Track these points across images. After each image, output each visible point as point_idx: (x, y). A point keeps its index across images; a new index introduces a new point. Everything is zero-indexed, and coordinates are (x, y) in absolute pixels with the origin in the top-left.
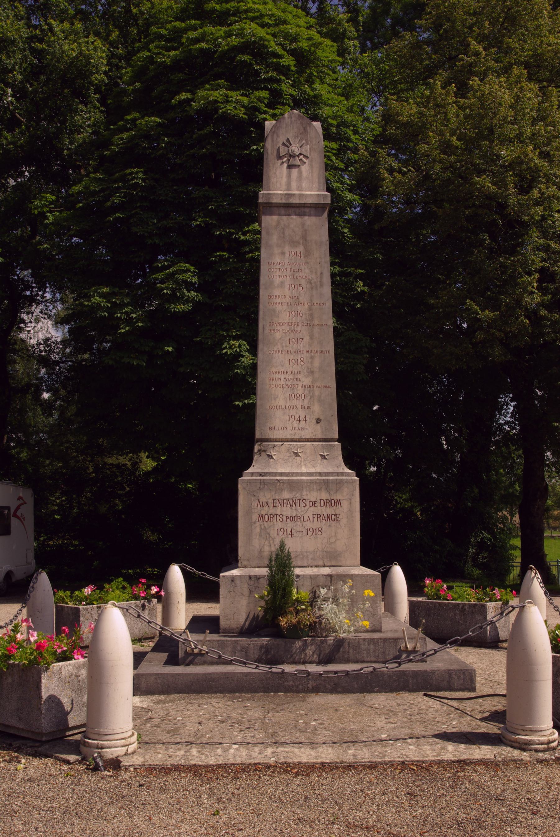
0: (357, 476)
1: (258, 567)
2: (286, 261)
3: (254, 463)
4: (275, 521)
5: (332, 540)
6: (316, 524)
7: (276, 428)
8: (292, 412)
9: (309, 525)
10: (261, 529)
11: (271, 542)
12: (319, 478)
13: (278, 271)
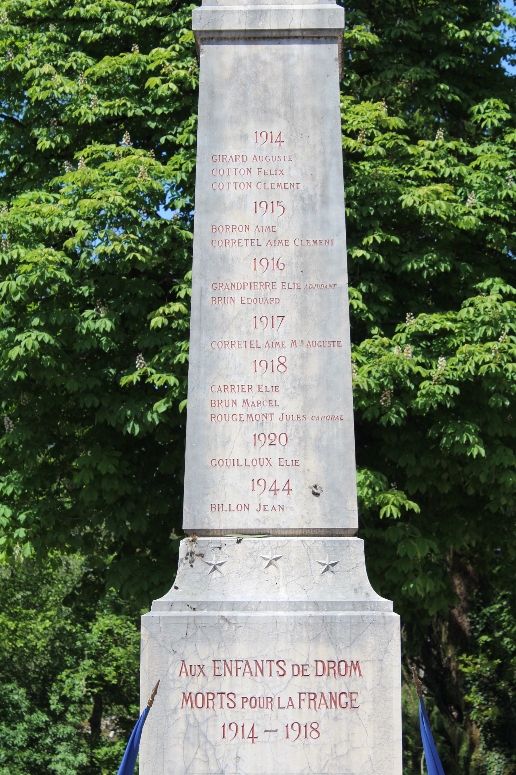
0: (395, 610)
3: (176, 583)
4: (217, 706)
5: (342, 750)
6: (306, 715)
7: (226, 507)
8: (259, 473)
9: (291, 715)
10: (188, 724)
11: (210, 753)
12: (313, 613)
13: (232, 173)
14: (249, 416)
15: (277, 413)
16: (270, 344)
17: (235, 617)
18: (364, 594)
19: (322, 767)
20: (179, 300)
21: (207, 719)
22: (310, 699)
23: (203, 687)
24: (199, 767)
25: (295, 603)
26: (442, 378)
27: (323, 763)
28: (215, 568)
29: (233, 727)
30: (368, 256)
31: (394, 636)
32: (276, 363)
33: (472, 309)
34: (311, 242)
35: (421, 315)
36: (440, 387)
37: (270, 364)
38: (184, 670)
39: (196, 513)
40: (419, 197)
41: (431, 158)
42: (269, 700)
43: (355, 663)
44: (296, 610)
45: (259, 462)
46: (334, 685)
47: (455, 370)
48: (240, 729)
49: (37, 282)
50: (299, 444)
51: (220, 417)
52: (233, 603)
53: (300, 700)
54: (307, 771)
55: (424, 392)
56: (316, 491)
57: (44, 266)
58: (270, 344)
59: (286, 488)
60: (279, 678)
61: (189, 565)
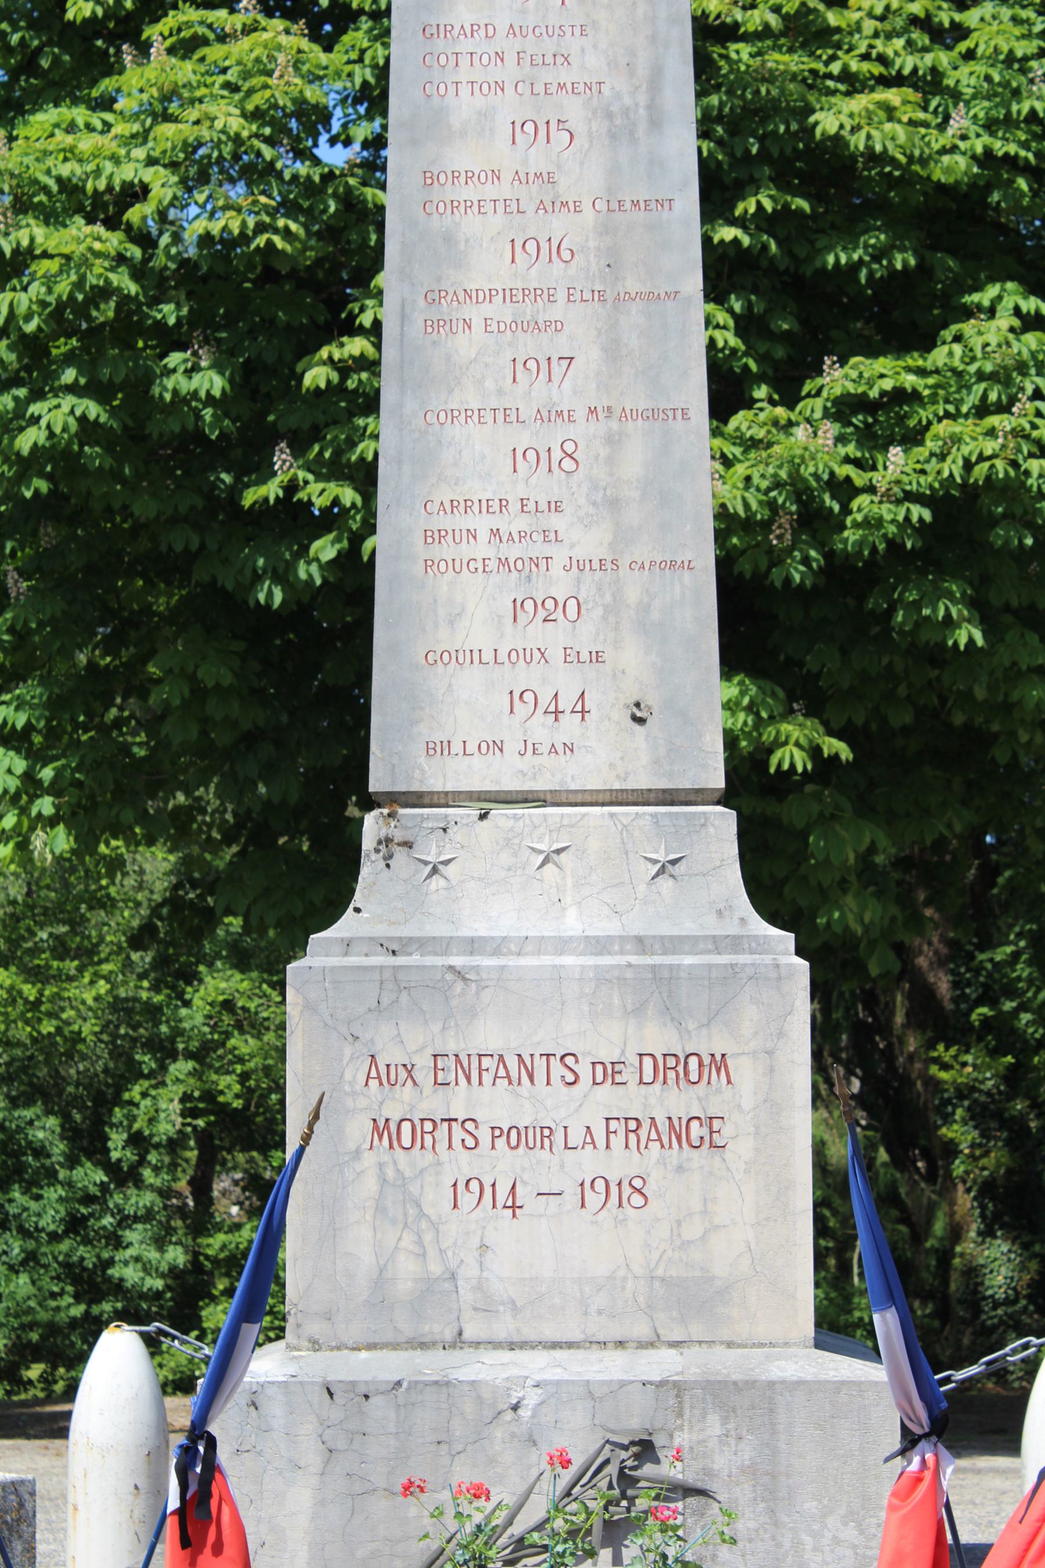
1: (371, 1347)
2: (502, 24)
3: (358, 900)
5: (692, 1231)
6: (620, 1162)
7: (457, 747)
8: (524, 677)
9: (589, 1163)
10: (383, 1181)
11: (428, 1237)
12: (634, 959)
14: (503, 562)
15: (560, 555)
16: (545, 414)
17: (477, 969)
18: (736, 921)
19: (653, 1264)
20: (361, 331)
21: (421, 1172)
22: (628, 1131)
23: (412, 1108)
24: (406, 1268)
25: (597, 939)
26: (896, 489)
27: (655, 1256)
28: (435, 870)
29: (474, 1185)
30: (746, 241)
31: (798, 1003)
32: (557, 454)
33: (957, 348)
34: (628, 205)
35: (854, 360)
36: (892, 507)
37: (544, 456)
38: (373, 1074)
39: (395, 760)
40: (851, 115)
41: (876, 35)
42: (546, 1132)
43: (718, 1058)
44: (600, 954)
45: (523, 656)
46: (676, 1102)
47: (923, 472)
48: (488, 1191)
49: (71, 297)
50: (605, 618)
51: (443, 564)
52: (472, 940)
53: (608, 1132)
54: (622, 1273)
55: (859, 518)
56: (639, 714)
57: (85, 262)
58: (545, 414)
59: (579, 708)
60: (565, 1089)
61: (382, 864)
